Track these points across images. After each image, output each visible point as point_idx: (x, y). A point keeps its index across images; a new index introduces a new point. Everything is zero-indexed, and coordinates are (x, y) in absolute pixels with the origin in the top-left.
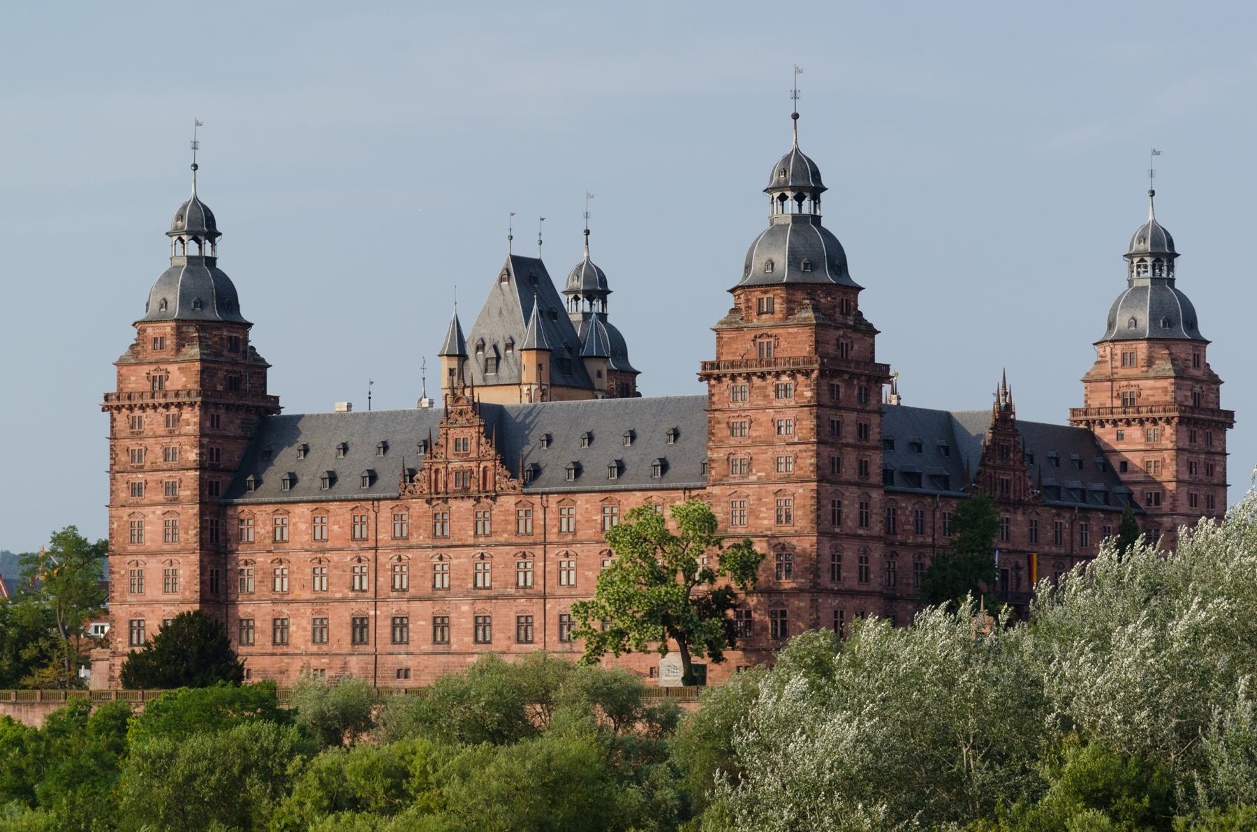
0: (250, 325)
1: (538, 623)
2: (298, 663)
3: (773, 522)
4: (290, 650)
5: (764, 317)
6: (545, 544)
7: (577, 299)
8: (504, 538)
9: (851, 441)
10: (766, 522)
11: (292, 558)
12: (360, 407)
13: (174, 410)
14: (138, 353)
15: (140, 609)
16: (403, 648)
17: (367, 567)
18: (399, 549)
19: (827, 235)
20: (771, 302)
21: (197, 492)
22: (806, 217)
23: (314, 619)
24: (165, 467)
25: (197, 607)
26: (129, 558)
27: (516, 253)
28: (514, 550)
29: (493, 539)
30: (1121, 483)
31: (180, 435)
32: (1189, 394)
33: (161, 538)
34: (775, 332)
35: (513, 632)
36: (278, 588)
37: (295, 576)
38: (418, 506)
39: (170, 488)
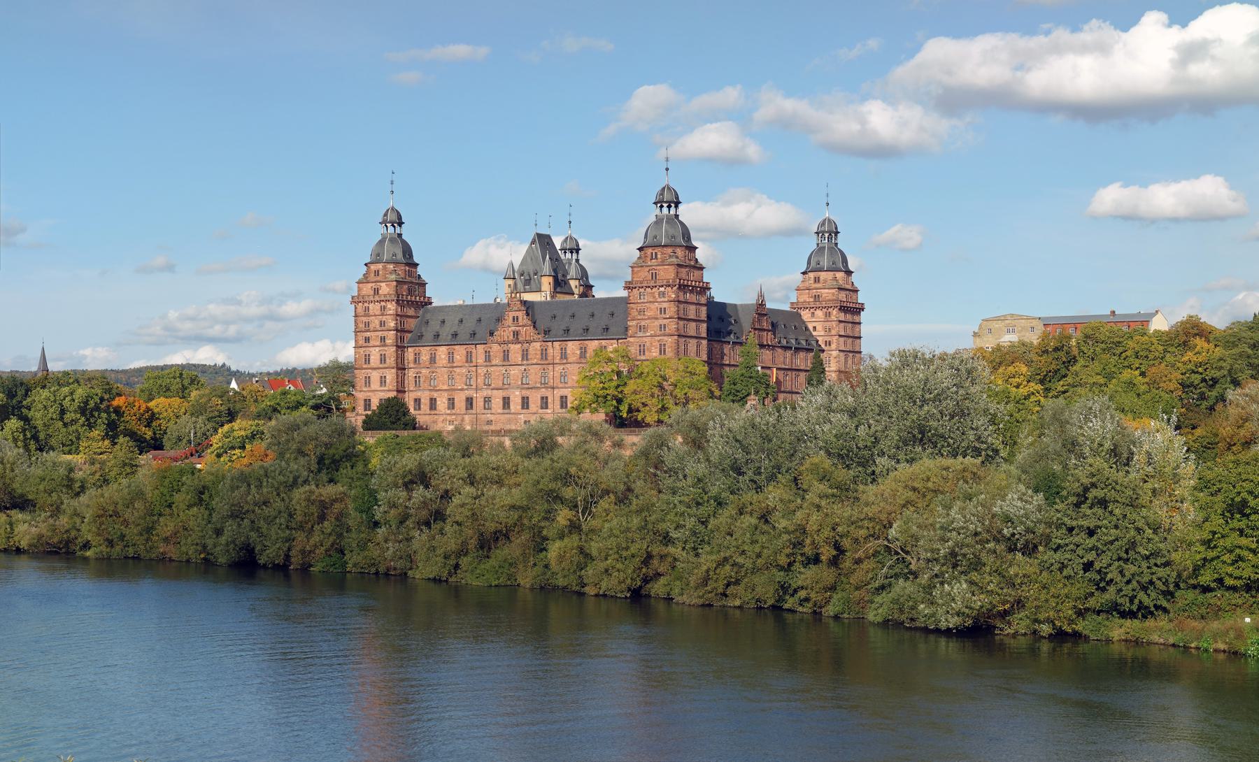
0: (418, 265)
1: (549, 400)
2: (441, 418)
3: (658, 354)
4: (437, 412)
5: (653, 261)
7: (565, 252)
8: (535, 361)
9: (692, 317)
10: (654, 354)
11: (438, 370)
12: (469, 302)
13: (383, 304)
14: (367, 277)
15: (370, 394)
16: (489, 411)
17: (474, 374)
18: (487, 366)
19: (681, 223)
20: (656, 253)
21: (395, 341)
22: (672, 215)
25: (395, 393)
27: (538, 232)
28: (539, 367)
30: (813, 336)
31: (386, 315)
32: (845, 296)
33: (379, 361)
34: (658, 267)
35: (539, 404)
36: (432, 384)
38: (495, 347)
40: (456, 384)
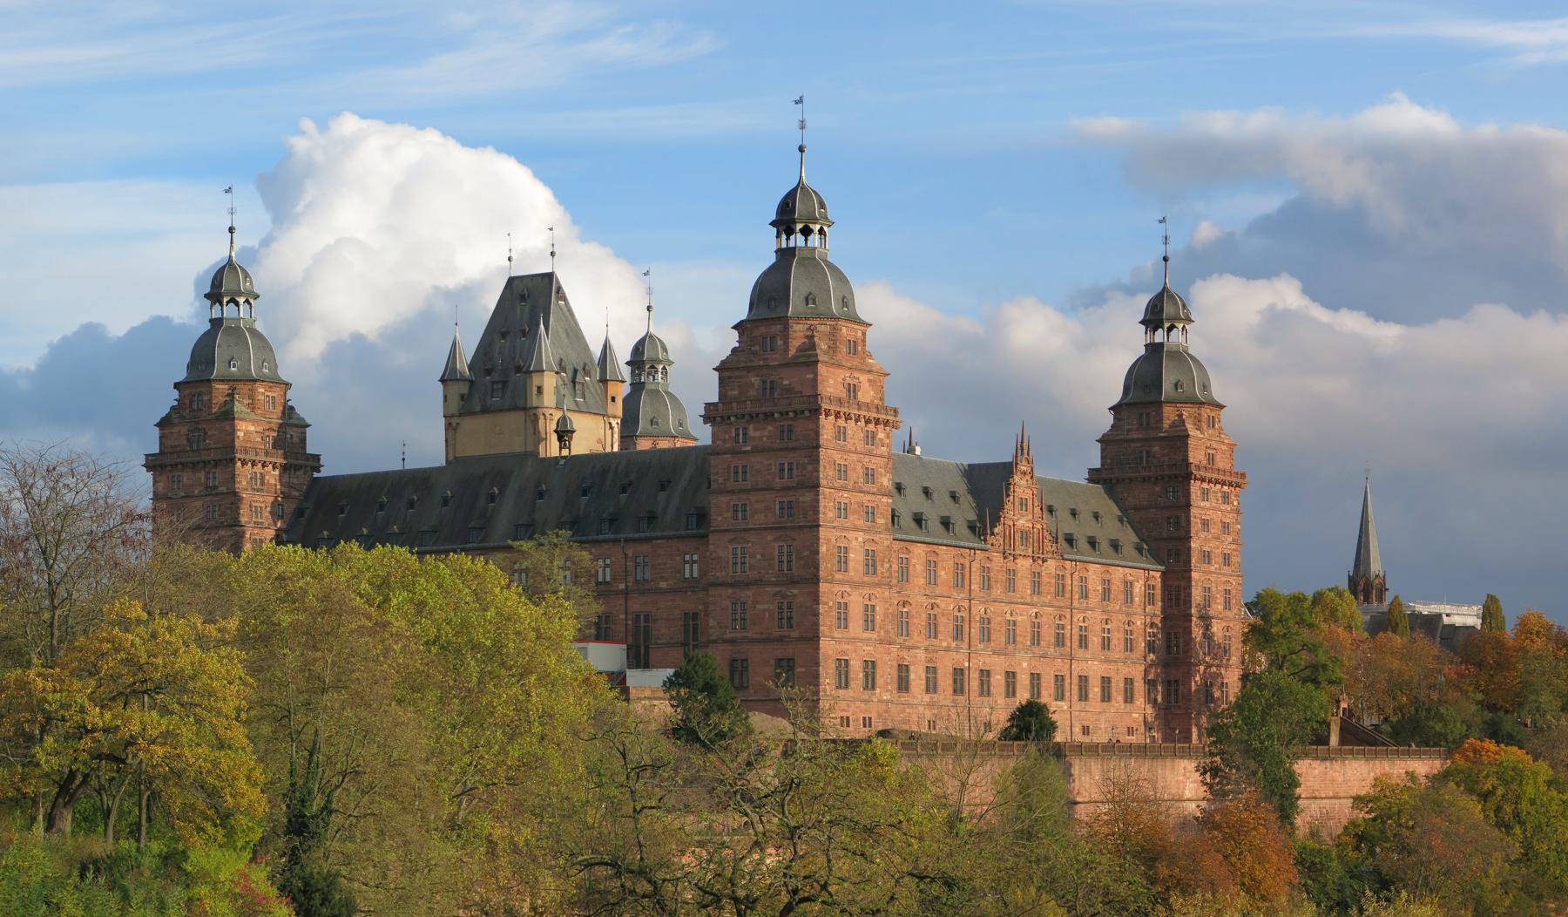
1: (1067, 681)
13: (871, 427)
15: (846, 647)
17: (964, 614)
24: (865, 489)
26: (837, 588)
33: (861, 568)
38: (997, 557)
39: (871, 513)
40: (940, 637)
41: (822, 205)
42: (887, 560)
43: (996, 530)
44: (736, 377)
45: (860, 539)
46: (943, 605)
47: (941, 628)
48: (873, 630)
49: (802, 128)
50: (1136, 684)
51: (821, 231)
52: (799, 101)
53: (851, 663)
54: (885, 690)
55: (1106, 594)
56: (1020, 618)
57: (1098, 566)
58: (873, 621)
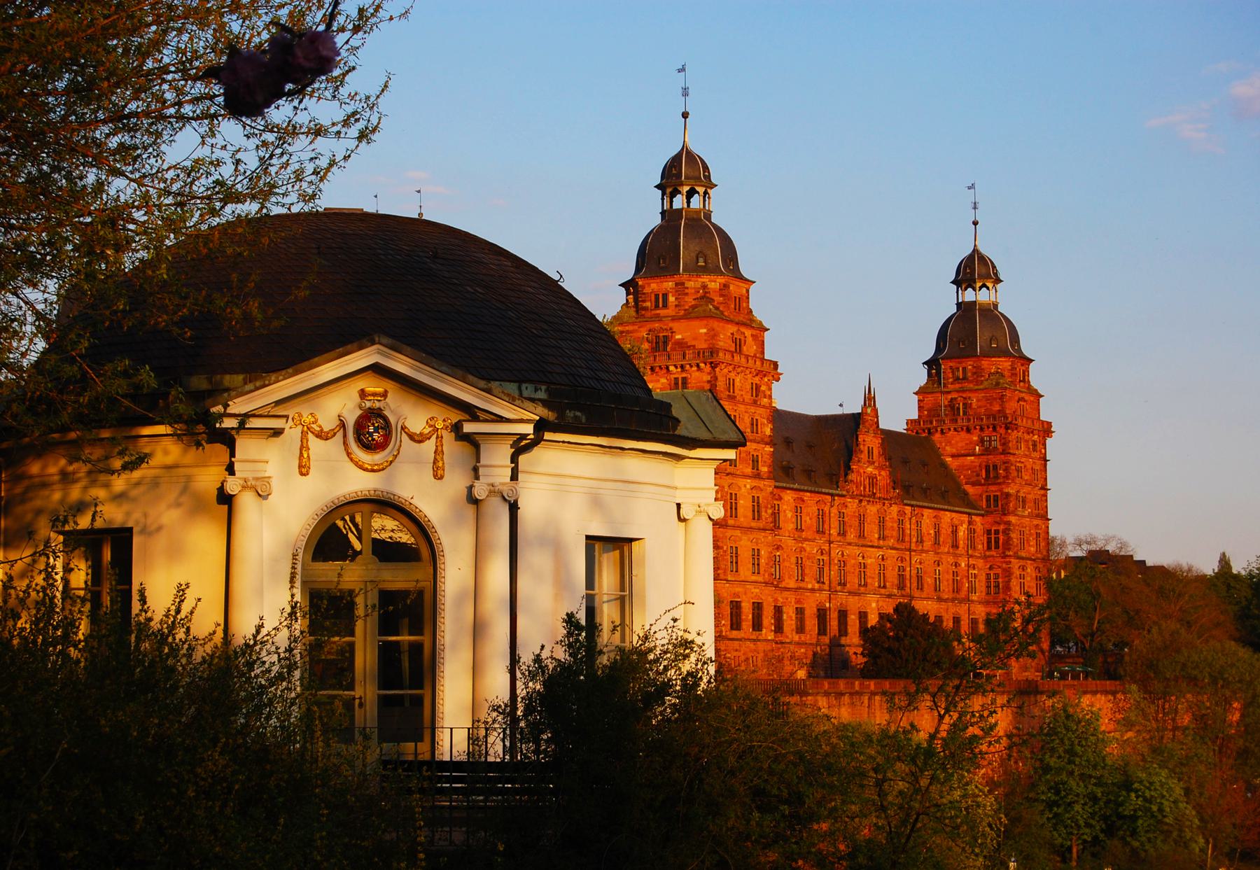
5: (1022, 384)
6: (910, 550)
8: (891, 542)
17: (825, 558)
23: (797, 608)
29: (886, 543)
33: (750, 514)
37: (787, 564)
38: (852, 505)
40: (807, 579)
41: (706, 168)
42: (769, 506)
43: (850, 477)
44: (628, 332)
45: (748, 486)
46: (808, 549)
47: (807, 571)
48: (758, 573)
49: (685, 92)
50: (962, 623)
51: (706, 193)
52: (682, 70)
53: (743, 604)
54: (768, 633)
55: (937, 534)
56: (869, 561)
57: (930, 511)
58: (758, 565)
